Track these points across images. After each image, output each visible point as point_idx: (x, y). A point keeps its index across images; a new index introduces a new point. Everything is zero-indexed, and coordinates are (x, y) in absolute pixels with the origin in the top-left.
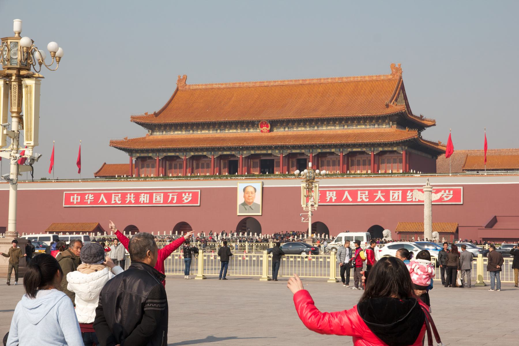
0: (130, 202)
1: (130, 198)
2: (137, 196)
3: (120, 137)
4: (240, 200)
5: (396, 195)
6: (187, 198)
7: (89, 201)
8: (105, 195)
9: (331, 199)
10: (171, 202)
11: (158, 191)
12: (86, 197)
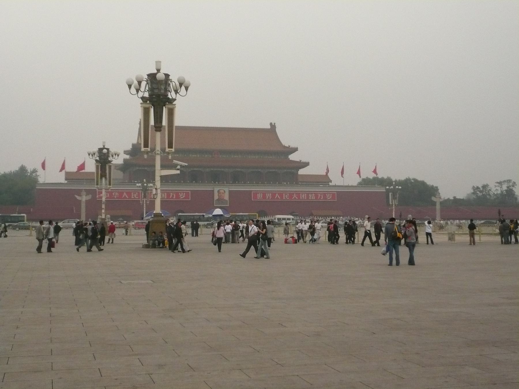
4: (216, 197)
5: (303, 196)
7: (115, 197)
8: (127, 193)
9: (269, 197)
10: (172, 198)
12: (113, 194)
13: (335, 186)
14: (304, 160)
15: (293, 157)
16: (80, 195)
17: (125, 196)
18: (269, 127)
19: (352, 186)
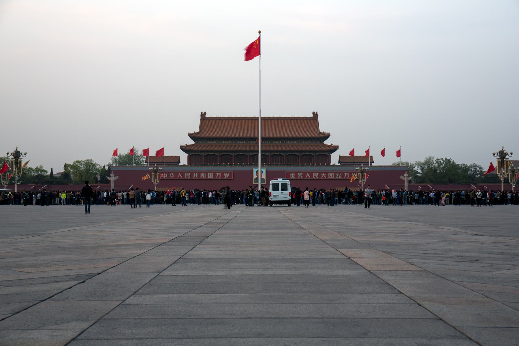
0: (195, 177)
1: (195, 175)
2: (199, 174)
3: (184, 144)
5: (331, 175)
6: (226, 176)
10: (218, 177)
11: (211, 172)
13: (382, 167)
14: (335, 144)
15: (327, 142)
16: (110, 176)
17: (180, 177)
18: (312, 116)
19: (389, 167)
